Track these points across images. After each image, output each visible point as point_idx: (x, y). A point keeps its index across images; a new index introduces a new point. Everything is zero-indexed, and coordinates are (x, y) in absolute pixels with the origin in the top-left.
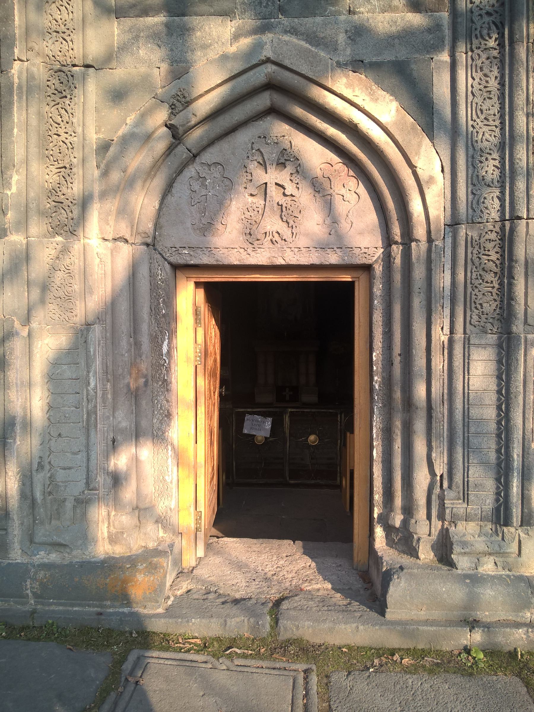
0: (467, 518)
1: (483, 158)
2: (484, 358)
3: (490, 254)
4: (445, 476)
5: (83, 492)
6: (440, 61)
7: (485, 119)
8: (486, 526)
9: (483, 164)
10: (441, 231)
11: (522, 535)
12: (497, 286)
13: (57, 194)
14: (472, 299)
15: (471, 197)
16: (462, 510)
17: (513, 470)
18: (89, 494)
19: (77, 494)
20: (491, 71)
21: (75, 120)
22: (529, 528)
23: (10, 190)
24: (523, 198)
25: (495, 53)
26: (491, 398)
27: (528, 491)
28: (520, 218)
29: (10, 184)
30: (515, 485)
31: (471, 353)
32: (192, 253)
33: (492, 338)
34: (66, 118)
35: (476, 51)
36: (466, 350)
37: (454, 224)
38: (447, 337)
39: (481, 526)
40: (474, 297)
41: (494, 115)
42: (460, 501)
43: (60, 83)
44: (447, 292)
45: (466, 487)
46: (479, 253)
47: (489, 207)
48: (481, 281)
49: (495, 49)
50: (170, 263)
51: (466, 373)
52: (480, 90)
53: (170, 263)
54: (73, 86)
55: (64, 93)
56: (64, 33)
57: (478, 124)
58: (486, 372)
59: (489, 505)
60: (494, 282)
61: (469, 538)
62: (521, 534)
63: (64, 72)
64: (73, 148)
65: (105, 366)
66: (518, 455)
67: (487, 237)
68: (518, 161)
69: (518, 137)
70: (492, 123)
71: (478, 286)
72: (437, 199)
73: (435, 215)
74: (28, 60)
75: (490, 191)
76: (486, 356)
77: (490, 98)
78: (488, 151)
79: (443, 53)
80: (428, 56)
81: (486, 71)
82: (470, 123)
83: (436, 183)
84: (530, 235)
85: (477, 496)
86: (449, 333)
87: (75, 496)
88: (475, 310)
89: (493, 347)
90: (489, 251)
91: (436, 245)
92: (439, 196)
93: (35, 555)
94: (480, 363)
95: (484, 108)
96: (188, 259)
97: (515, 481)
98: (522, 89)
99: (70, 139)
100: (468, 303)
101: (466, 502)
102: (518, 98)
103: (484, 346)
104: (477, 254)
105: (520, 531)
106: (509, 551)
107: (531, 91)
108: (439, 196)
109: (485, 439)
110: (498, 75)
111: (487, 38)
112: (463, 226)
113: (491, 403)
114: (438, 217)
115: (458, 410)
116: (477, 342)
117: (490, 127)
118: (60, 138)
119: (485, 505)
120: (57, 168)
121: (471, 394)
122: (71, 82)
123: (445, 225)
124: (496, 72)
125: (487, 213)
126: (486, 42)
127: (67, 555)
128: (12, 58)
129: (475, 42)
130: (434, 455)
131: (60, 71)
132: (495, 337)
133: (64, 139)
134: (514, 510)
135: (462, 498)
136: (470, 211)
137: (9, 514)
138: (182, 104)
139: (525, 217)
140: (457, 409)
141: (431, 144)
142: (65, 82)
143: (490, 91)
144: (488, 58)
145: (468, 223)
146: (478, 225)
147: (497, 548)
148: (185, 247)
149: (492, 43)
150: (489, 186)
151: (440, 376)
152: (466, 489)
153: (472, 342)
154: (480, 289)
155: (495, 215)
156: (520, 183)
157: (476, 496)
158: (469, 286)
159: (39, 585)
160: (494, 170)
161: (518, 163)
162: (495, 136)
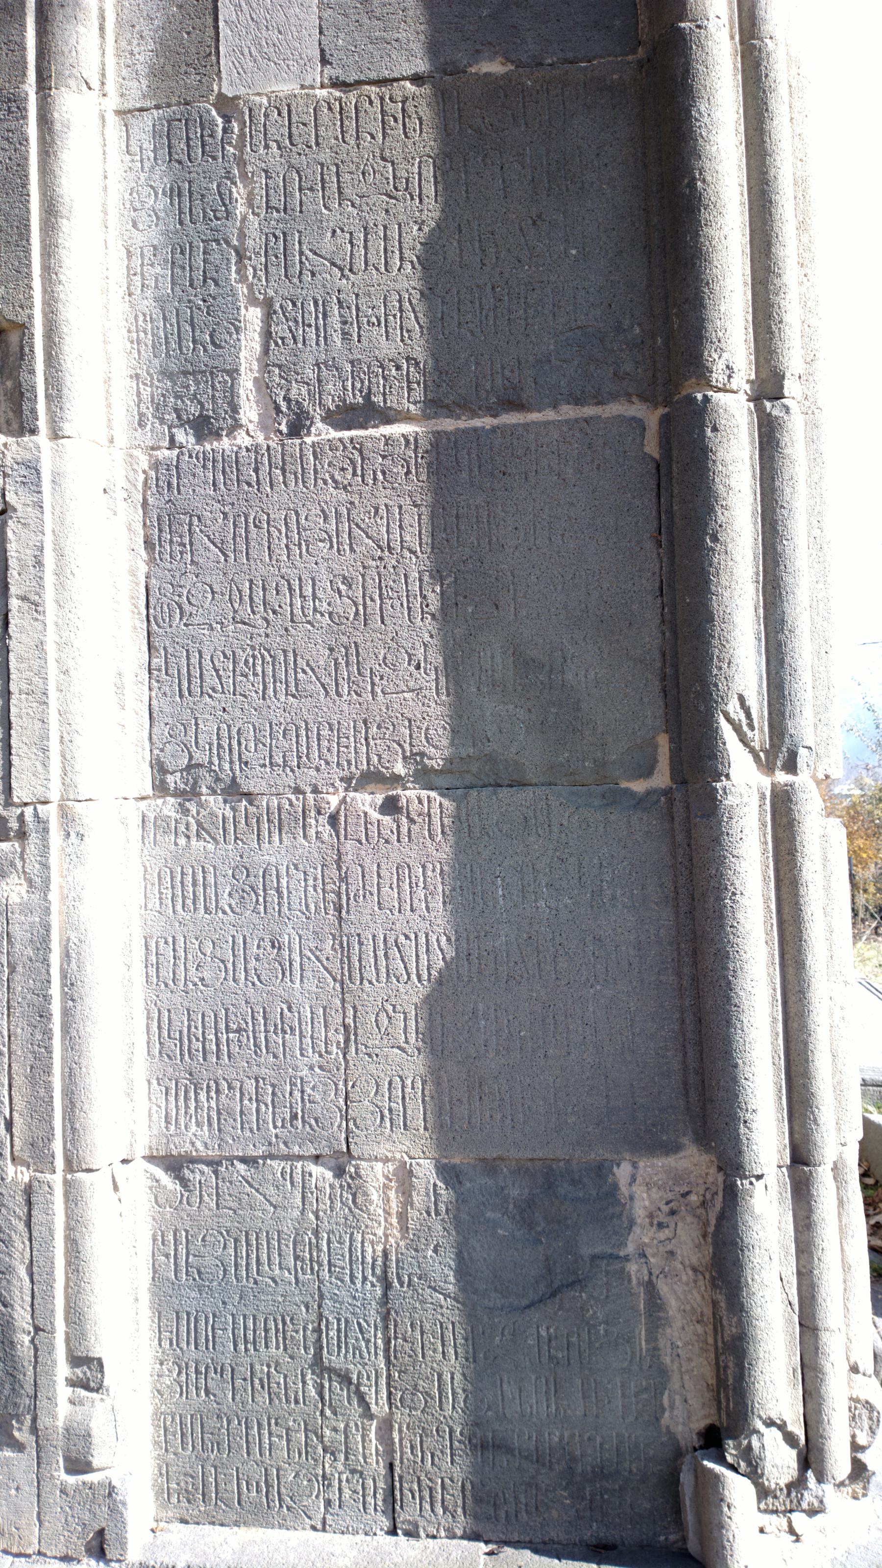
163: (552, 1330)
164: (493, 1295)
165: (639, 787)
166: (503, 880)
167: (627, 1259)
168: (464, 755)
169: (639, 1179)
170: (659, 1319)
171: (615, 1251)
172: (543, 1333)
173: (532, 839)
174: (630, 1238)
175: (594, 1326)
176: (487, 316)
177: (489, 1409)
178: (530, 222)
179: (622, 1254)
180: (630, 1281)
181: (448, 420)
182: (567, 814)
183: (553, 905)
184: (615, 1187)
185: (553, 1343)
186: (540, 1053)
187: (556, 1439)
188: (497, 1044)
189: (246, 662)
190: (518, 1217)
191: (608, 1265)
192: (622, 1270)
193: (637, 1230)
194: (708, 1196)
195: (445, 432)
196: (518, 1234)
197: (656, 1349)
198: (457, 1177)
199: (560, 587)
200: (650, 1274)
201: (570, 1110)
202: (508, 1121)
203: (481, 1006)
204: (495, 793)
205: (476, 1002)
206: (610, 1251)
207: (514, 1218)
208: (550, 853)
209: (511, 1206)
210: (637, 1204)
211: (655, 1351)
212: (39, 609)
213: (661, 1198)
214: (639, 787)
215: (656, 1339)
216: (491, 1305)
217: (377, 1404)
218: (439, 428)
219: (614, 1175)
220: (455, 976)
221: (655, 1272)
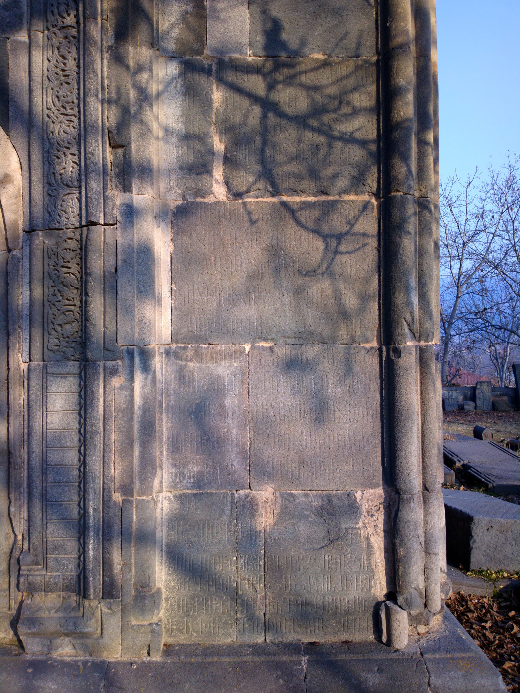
0: (48, 588)
1: (59, 153)
2: (64, 390)
3: (69, 266)
4: (26, 536)
6: (16, 41)
7: (63, 107)
8: (69, 597)
9: (60, 160)
10: (19, 239)
11: (105, 610)
12: (78, 304)
14: (49, 319)
15: (47, 198)
16: (39, 578)
17: (89, 529)
20: (69, 52)
22: (112, 601)
24: (98, 200)
25: (74, 32)
26: (72, 439)
27: (109, 554)
28: (95, 224)
30: (91, 546)
31: (48, 384)
33: (74, 365)
35: (52, 29)
36: (45, 380)
37: (30, 231)
38: (27, 364)
39: (63, 598)
40: (51, 316)
41: (73, 103)
42: (40, 567)
44: (26, 312)
45: (45, 549)
46: (57, 264)
47: (67, 211)
48: (61, 298)
49: (74, 28)
51: (44, 408)
52: (57, 74)
57: (53, 113)
58: (67, 407)
59: (72, 571)
60: (75, 299)
61: (44, 614)
62: (103, 609)
66: (95, 510)
67: (66, 246)
68: (90, 156)
69: (90, 128)
70: (70, 111)
71: (57, 303)
72: (14, 200)
73: (11, 219)
75: (67, 192)
76: (66, 387)
77: (68, 83)
78: (67, 145)
79: (21, 32)
80: (4, 36)
81: (63, 51)
82: (46, 111)
83: (13, 182)
84: (107, 244)
85: (57, 560)
86: (28, 360)
88: (53, 332)
89: (75, 377)
90: (69, 262)
91: (13, 255)
92: (16, 197)
94: (59, 396)
95: (61, 94)
97: (92, 541)
98: (94, 72)
100: (46, 324)
101: (45, 567)
102: (89, 82)
103: (64, 376)
104: (54, 266)
105: (102, 604)
106: (86, 630)
107: (105, 74)
108: (16, 197)
109: (66, 489)
110: (76, 57)
111: (65, 15)
112: (40, 233)
113: (72, 444)
114: (15, 223)
115: (34, 454)
116: (55, 370)
117: (67, 117)
119: (67, 572)
121: (48, 434)
123: (24, 231)
124: (74, 54)
125: (67, 218)
126: (64, 20)
129: (51, 18)
130: (12, 509)
132: (77, 364)
134: (91, 579)
135: (41, 562)
136: (47, 215)
139: (103, 223)
140: (33, 452)
141: (6, 137)
143: (68, 76)
144: (66, 37)
145: (46, 230)
146: (57, 232)
147: (71, 628)
149: (70, 20)
150: (68, 186)
151: (20, 412)
152: (45, 552)
153: (49, 371)
154: (59, 308)
155: (74, 220)
156: (93, 182)
157: (56, 560)
158: (47, 304)
160: (73, 167)
161: (90, 158)
162: (74, 128)
163: (330, 557)
164: (307, 544)
165: (367, 346)
166: (314, 381)
167: (359, 528)
168: (300, 331)
169: (364, 498)
170: (371, 551)
171: (355, 526)
172: (326, 558)
173: (326, 365)
174: (360, 520)
175: (346, 555)
176: (314, 157)
177: (304, 589)
178: (332, 120)
179: (357, 526)
180: (360, 537)
181: (297, 197)
182: (340, 356)
183: (334, 391)
184: (355, 501)
185: (330, 562)
186: (327, 449)
187: (331, 600)
188: (311, 446)
189: (212, 291)
190: (316, 513)
191: (352, 531)
192: (357, 533)
193: (362, 517)
194: (391, 503)
195: (296, 202)
196: (317, 520)
197: (370, 563)
198: (293, 498)
199: (340, 266)
200: (368, 534)
201: (338, 471)
202: (314, 476)
203: (304, 431)
204: (312, 347)
205: (302, 429)
206: (352, 526)
207: (315, 514)
208: (333, 371)
209: (314, 509)
210: (363, 507)
211: (369, 564)
212: (131, 265)
213: (373, 505)
214: (367, 346)
215: (370, 559)
216: (306, 547)
217: (260, 589)
218: (294, 200)
219: (355, 496)
220: (294, 419)
221: (370, 533)
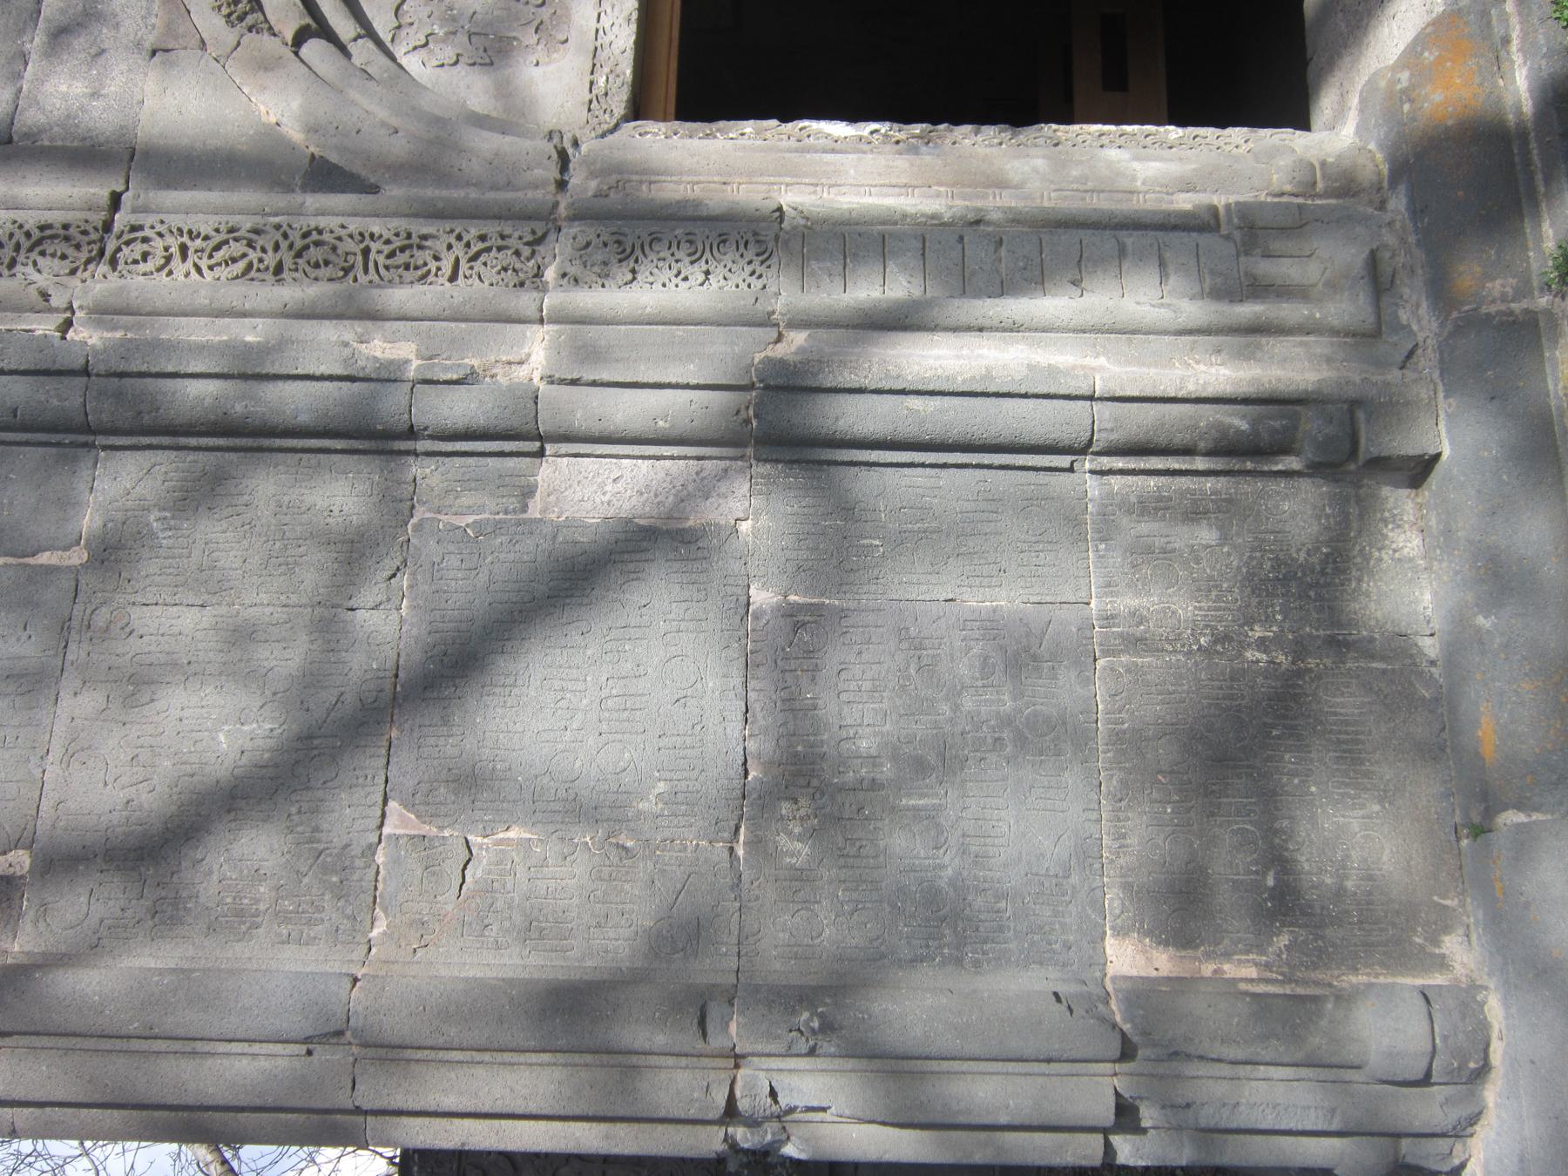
5: (1228, 237)
13: (434, 270)
18: (1230, 221)
19: (1230, 249)
21: (248, 226)
23: (407, 361)
29: (391, 362)
32: (606, 70)
34: (236, 248)
43: (145, 260)
50: (627, 119)
53: (627, 119)
54: (159, 228)
55: (172, 250)
56: (18, 247)
63: (119, 249)
64: (320, 232)
65: (891, 190)
74: (70, 308)
87: (1238, 255)
93: (1412, 333)
96: (619, 81)
99: (295, 236)
118: (288, 262)
120: (366, 271)
122: (148, 233)
127: (1401, 259)
128: (57, 342)
131: (113, 263)
133: (293, 253)
137: (1306, 391)
138: (252, 11)
142: (145, 247)
148: (592, 83)
159: (1494, 279)
